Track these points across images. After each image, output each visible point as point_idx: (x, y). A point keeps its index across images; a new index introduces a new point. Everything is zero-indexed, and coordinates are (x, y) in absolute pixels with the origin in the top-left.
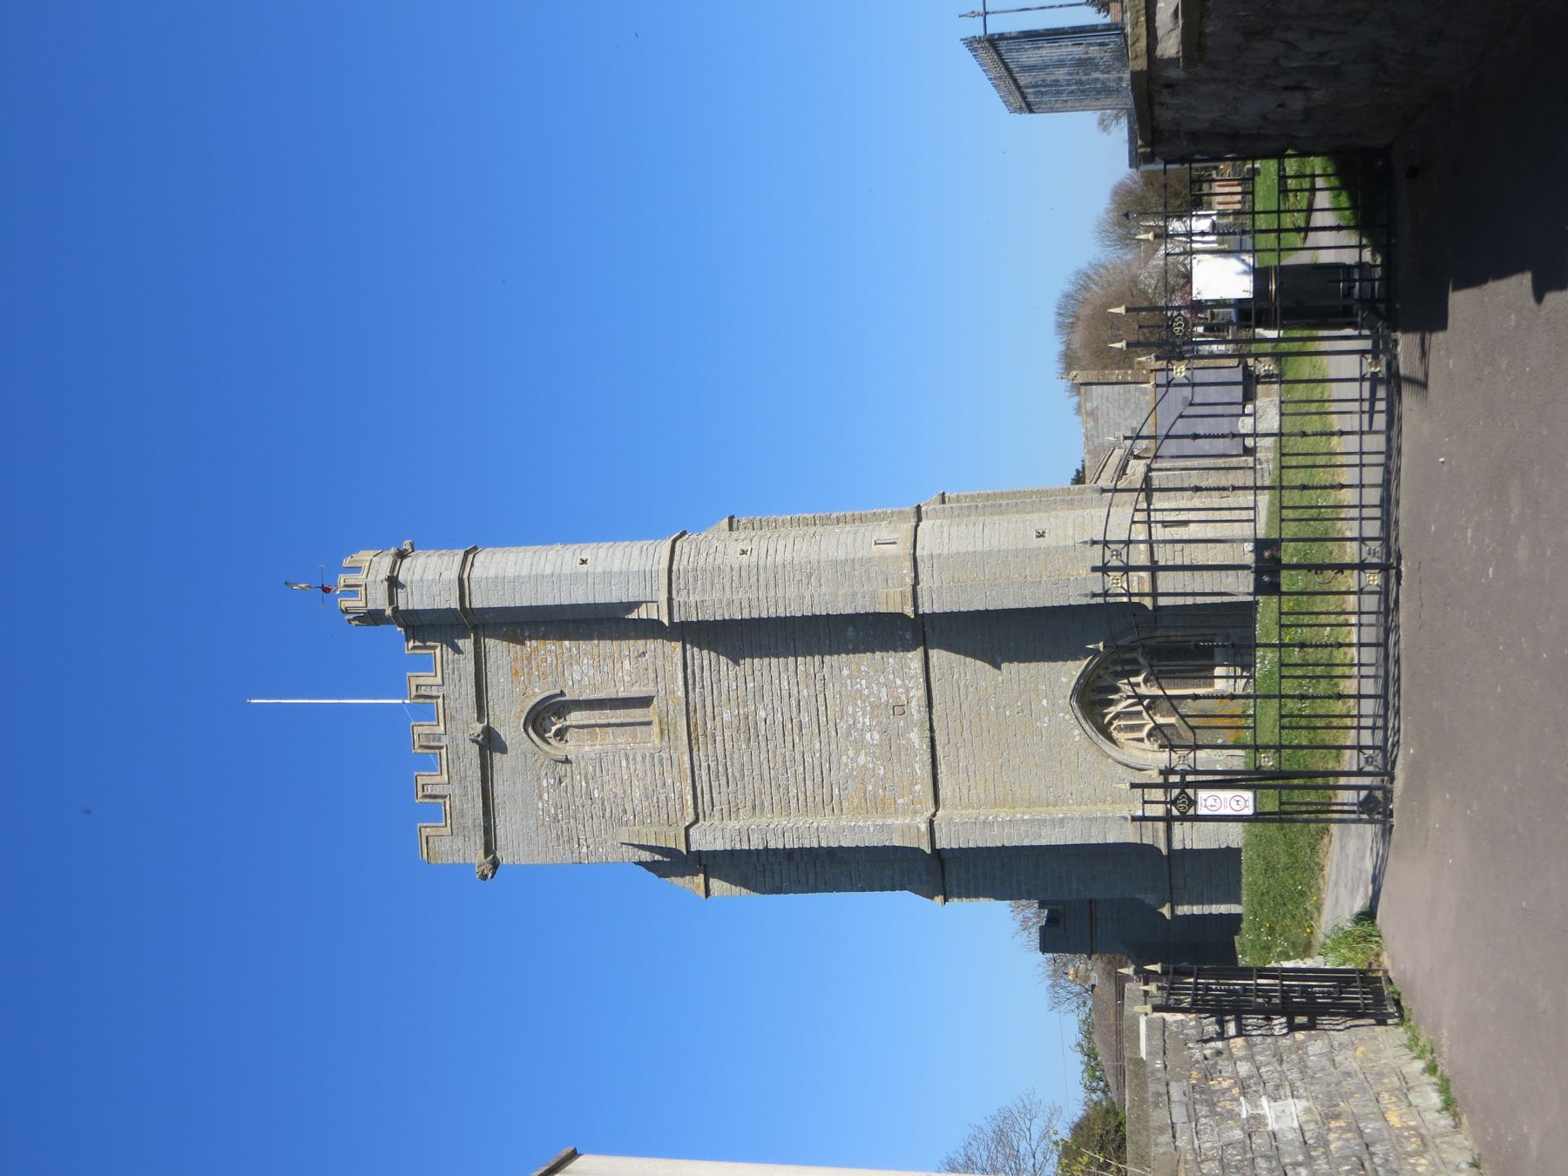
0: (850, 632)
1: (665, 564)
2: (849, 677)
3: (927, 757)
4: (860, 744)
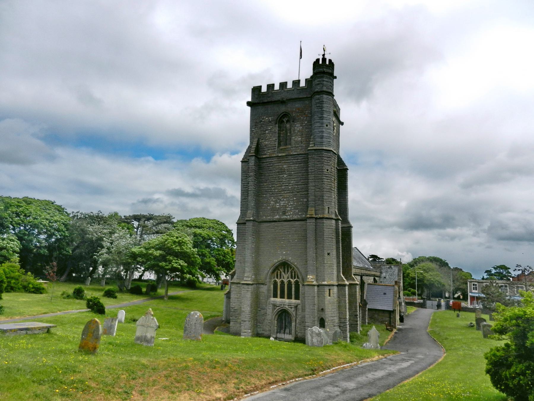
0: (305, 200)
1: (324, 148)
2: (294, 200)
3: (271, 220)
4: (276, 202)
